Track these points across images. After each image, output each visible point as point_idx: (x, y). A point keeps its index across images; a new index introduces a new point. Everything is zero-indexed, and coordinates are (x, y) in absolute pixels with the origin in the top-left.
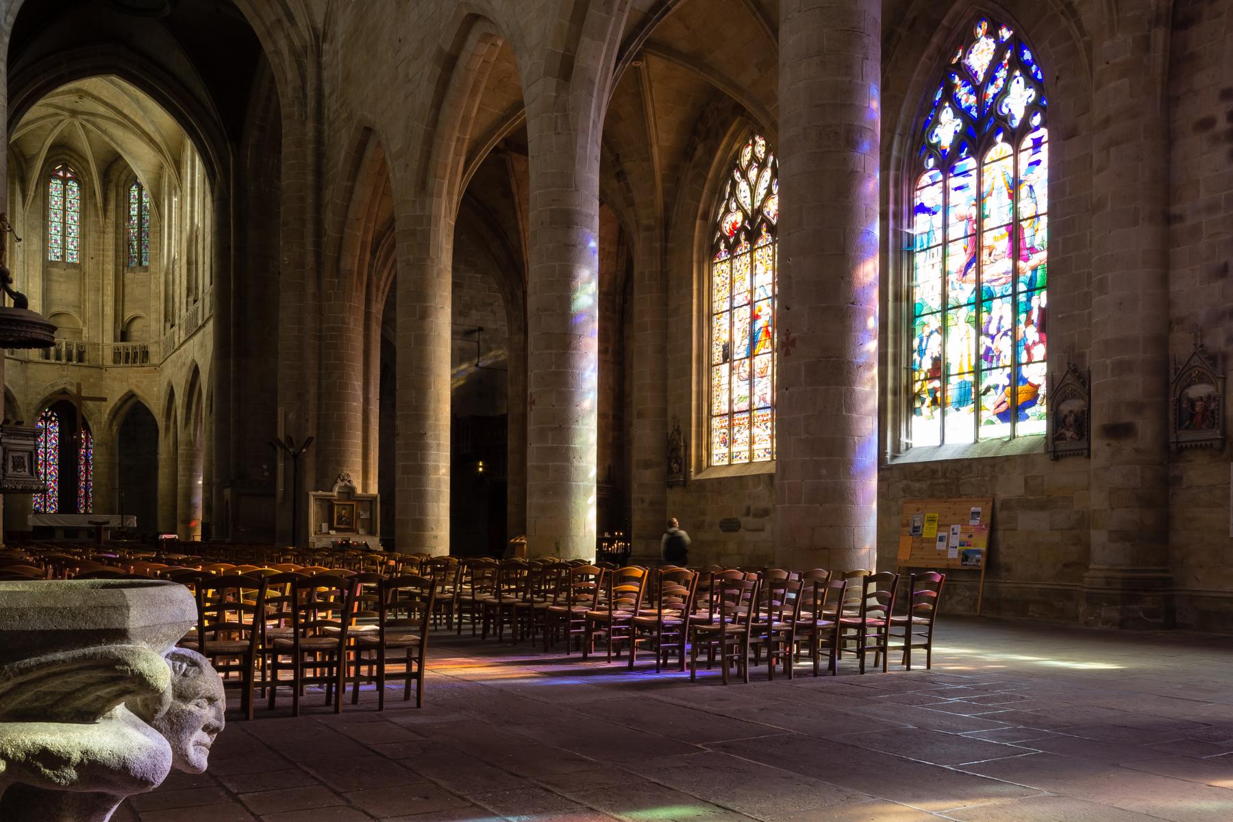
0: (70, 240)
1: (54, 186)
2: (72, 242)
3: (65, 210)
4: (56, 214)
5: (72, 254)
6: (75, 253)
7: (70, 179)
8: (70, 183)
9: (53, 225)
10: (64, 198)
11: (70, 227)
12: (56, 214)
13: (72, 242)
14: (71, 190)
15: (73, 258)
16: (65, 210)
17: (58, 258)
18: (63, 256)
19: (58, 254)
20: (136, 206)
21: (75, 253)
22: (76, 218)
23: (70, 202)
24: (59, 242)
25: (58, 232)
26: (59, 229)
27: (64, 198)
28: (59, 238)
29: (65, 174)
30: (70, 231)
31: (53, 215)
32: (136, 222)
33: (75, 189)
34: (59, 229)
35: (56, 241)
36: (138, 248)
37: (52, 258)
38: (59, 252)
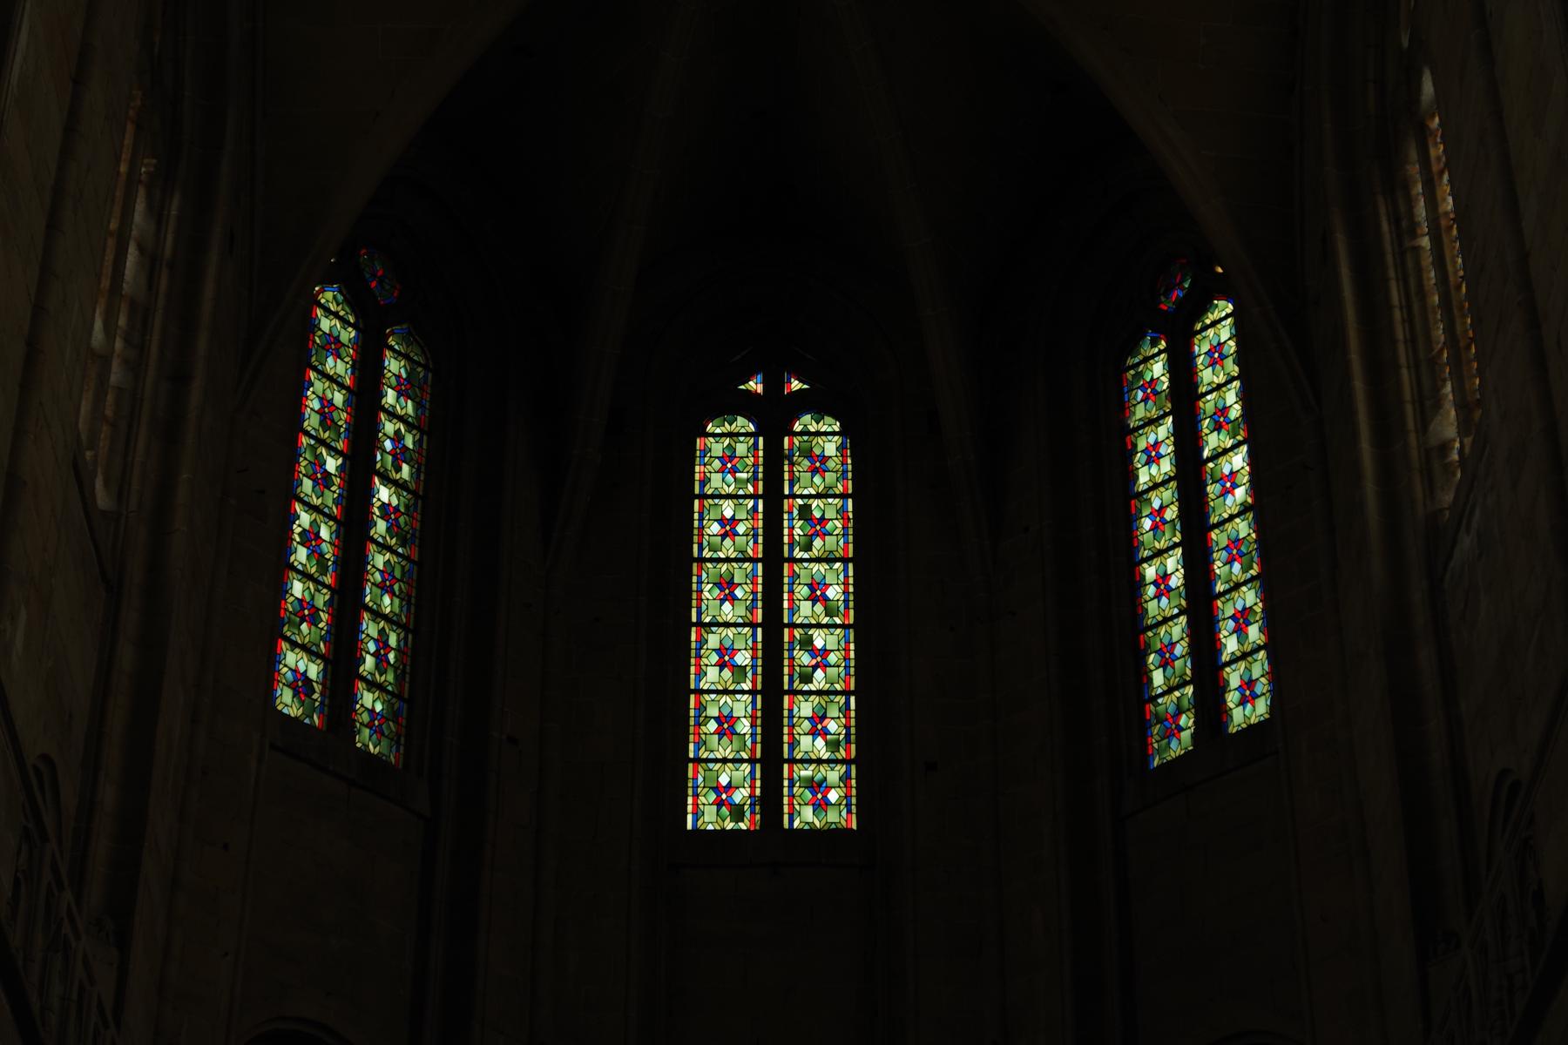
0: (805, 708)
1: (717, 448)
2: (818, 718)
3: (774, 559)
4: (726, 587)
5: (816, 786)
6: (833, 775)
7: (801, 403)
8: (806, 422)
9: (713, 641)
10: (773, 497)
11: (807, 643)
12: (726, 587)
13: (818, 718)
14: (808, 454)
15: (821, 805)
16: (774, 559)
17: (737, 812)
18: (770, 799)
19: (739, 796)
20: (1164, 430)
21: (833, 775)
22: (834, 593)
23: (805, 512)
24: (744, 727)
25: (739, 671)
26: (743, 658)
27: (773, 497)
28: (741, 707)
29: (774, 384)
30: (805, 659)
31: (709, 592)
32: (1171, 513)
33: (830, 447)
34: (743, 658)
35: (726, 724)
36: (1195, 651)
37: (707, 816)
38: (742, 783)
